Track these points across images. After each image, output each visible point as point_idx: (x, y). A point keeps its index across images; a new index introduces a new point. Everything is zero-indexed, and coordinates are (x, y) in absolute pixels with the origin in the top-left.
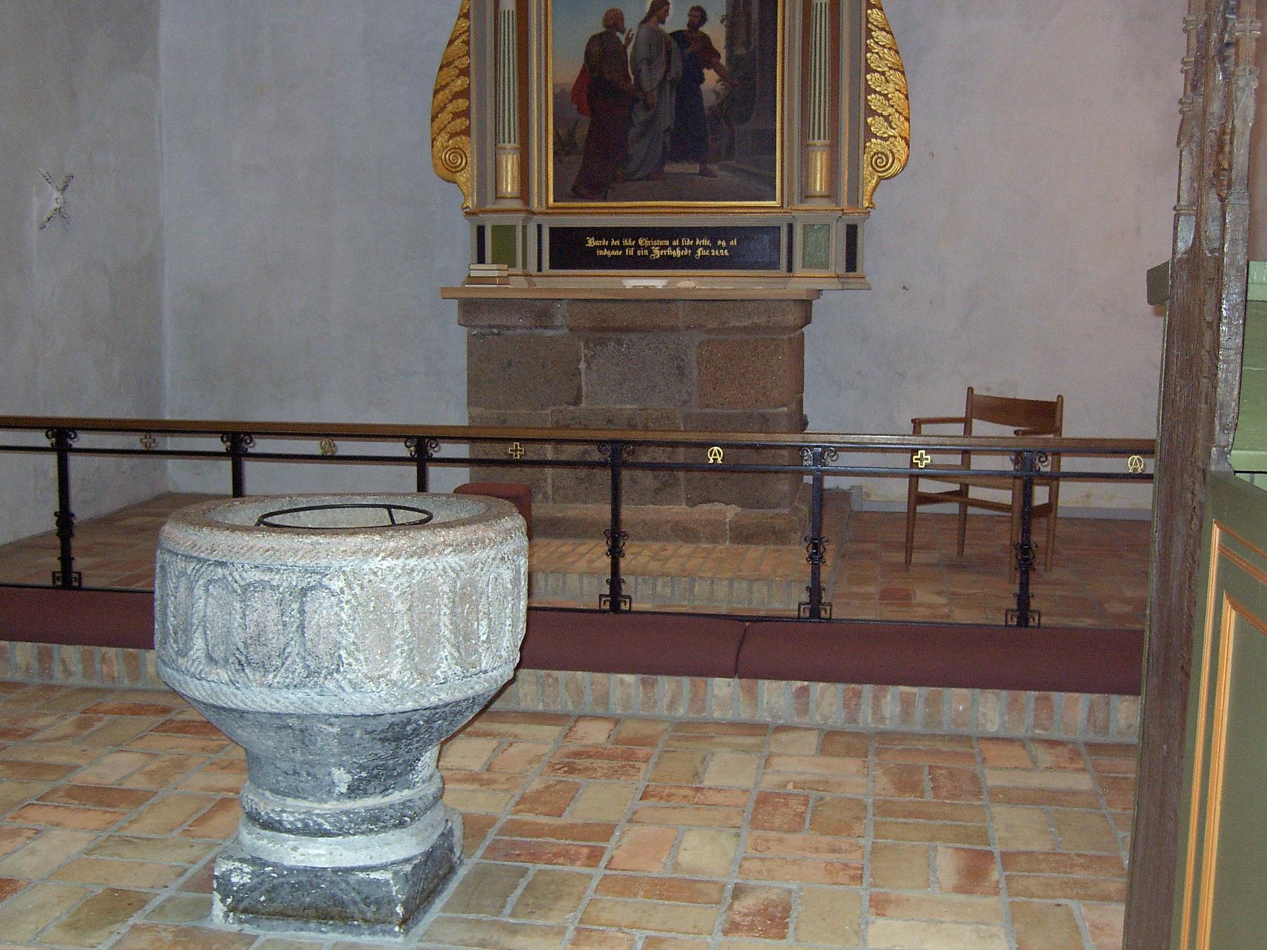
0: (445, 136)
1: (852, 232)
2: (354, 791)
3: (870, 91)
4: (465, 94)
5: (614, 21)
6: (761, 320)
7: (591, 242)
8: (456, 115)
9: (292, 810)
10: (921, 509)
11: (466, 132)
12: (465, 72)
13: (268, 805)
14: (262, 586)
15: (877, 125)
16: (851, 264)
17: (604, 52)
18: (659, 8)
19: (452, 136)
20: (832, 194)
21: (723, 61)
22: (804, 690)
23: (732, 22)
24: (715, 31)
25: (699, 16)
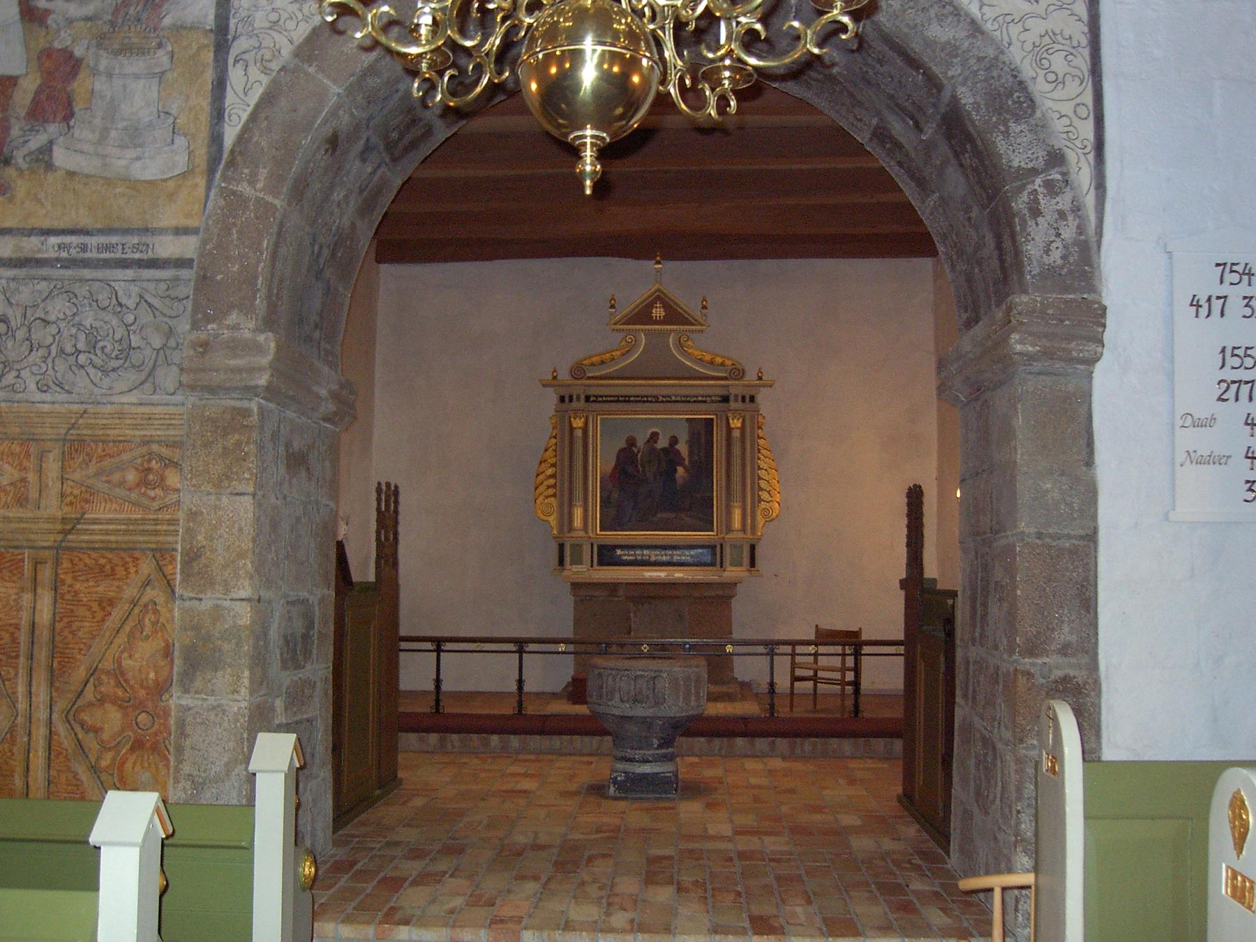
0: (541, 498)
1: (753, 548)
2: (660, 747)
3: (760, 478)
4: (553, 476)
5: (631, 442)
6: (720, 593)
7: (619, 552)
8: (549, 487)
9: (638, 754)
10: (797, 684)
11: (554, 495)
12: (553, 465)
13: (629, 753)
14: (642, 676)
15: (764, 495)
16: (753, 563)
17: (626, 457)
18: (654, 436)
19: (547, 497)
20: (744, 530)
21: (687, 463)
22: (773, 742)
23: (691, 443)
24: (682, 448)
25: (674, 441)
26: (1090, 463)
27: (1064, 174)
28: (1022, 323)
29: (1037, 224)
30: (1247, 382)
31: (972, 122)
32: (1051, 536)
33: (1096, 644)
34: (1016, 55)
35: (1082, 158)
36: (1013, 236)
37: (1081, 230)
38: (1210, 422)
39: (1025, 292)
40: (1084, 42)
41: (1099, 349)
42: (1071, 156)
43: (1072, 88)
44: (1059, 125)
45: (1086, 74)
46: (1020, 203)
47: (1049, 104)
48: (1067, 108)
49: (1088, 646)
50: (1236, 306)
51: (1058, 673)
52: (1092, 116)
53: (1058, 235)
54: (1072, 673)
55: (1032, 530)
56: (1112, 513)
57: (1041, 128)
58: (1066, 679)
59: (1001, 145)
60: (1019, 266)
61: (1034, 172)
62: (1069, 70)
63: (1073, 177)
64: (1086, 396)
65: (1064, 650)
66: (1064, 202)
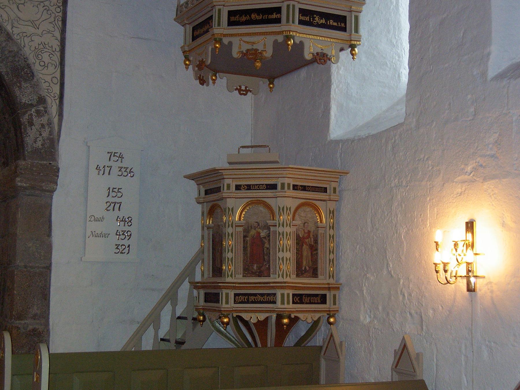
26: (49, 235)
27: (45, 108)
28: (22, 173)
29: (31, 129)
30: (118, 203)
31: (5, 81)
32: (31, 267)
33: (49, 314)
34: (27, 51)
35: (54, 102)
36: (21, 133)
37: (51, 133)
38: (101, 219)
39: (25, 160)
40: (58, 49)
41: (55, 187)
42: (49, 100)
43: (51, 69)
44: (44, 86)
45: (58, 64)
46: (25, 119)
47: (41, 76)
48: (48, 78)
49: (45, 315)
50: (115, 170)
51: (31, 327)
52: (59, 83)
53: (41, 135)
54: (37, 326)
55: (23, 264)
56: (58, 256)
57: (36, 86)
58: (34, 330)
59: (17, 92)
60: (23, 148)
61: (32, 105)
62: (50, 61)
63: (49, 109)
64: (49, 206)
65: (34, 317)
66: (44, 120)
